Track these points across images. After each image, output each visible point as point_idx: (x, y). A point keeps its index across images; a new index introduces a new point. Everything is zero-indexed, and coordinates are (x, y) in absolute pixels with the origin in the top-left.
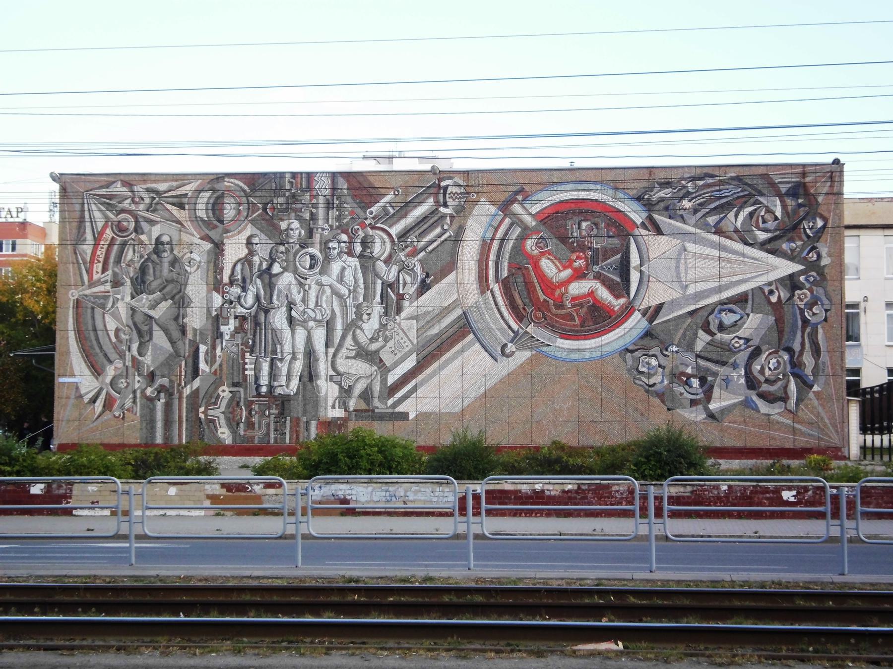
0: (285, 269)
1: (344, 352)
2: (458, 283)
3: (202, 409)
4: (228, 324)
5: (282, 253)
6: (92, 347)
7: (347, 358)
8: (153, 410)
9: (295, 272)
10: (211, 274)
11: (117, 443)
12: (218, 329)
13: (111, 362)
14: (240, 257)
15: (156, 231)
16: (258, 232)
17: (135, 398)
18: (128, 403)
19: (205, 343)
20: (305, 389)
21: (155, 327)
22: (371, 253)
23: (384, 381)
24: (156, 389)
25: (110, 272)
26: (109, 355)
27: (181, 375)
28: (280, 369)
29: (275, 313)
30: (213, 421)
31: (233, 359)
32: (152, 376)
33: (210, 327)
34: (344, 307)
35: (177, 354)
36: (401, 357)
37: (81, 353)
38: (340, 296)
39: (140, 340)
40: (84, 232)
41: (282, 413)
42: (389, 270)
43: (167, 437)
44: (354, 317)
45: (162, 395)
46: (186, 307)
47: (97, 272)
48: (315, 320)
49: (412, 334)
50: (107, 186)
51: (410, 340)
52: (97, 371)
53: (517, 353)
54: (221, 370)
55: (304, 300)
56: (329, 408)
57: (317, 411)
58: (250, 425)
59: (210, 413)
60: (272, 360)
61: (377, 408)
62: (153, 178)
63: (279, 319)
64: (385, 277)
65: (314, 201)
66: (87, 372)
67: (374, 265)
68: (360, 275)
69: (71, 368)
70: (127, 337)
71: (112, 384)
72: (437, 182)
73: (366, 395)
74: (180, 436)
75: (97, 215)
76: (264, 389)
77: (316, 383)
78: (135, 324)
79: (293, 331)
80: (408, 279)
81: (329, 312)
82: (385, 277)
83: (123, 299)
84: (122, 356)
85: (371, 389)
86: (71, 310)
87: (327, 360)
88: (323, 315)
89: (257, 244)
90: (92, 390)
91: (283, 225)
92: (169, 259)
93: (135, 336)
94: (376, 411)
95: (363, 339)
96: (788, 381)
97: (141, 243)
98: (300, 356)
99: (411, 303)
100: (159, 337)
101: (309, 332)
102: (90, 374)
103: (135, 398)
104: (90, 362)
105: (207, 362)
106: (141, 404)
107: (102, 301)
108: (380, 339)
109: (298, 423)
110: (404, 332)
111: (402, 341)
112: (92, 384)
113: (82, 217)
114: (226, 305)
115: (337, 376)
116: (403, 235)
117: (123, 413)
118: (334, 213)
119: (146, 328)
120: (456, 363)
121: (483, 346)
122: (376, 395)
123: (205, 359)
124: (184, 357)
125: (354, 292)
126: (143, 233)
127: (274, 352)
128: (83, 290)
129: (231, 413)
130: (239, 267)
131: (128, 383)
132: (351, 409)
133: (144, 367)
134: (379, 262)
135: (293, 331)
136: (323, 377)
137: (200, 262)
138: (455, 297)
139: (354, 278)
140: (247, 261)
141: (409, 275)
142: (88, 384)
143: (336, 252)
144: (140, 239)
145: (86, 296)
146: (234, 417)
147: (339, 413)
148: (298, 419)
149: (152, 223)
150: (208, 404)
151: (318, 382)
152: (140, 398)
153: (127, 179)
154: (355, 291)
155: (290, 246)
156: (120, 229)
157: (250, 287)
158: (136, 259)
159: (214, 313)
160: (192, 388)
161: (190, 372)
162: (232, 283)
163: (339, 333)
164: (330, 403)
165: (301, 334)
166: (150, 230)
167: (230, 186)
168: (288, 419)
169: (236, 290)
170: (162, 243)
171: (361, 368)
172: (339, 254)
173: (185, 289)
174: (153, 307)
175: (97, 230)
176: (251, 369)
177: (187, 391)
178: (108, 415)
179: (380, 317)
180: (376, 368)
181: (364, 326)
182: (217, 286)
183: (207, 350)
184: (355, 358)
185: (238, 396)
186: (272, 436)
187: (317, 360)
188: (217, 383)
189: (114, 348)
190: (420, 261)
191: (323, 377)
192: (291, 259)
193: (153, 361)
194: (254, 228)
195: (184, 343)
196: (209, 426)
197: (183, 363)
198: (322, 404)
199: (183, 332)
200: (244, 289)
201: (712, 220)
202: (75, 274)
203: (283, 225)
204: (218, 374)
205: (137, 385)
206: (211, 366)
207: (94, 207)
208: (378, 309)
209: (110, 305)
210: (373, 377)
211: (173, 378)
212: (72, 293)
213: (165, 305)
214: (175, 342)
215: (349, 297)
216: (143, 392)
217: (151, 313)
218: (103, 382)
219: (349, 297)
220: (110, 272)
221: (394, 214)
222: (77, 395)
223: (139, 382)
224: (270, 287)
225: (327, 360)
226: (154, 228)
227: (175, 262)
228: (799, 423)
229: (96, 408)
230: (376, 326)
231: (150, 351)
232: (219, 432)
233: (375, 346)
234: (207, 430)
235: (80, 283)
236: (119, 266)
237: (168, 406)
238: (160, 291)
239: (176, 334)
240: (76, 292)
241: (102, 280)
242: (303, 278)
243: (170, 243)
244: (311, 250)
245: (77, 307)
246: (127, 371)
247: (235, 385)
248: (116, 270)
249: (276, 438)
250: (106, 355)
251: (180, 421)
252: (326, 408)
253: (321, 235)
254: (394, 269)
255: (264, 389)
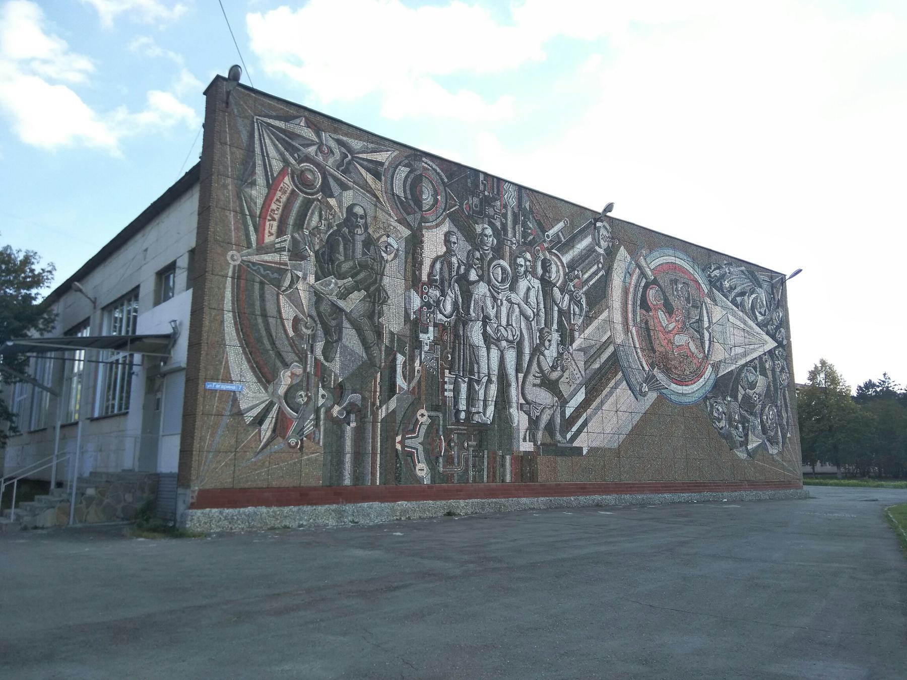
0: (481, 278)
1: (530, 378)
2: (609, 321)
3: (399, 438)
4: (427, 332)
5: (477, 259)
6: (259, 340)
7: (534, 385)
8: (341, 437)
9: (489, 283)
10: (409, 268)
11: (291, 485)
12: (418, 337)
13: (286, 365)
14: (439, 254)
15: (348, 197)
16: (455, 230)
17: (317, 419)
18: (309, 427)
19: (404, 354)
20: (500, 417)
21: (346, 324)
22: (550, 277)
23: (563, 413)
24: (344, 408)
25: (288, 237)
26: (284, 354)
27: (375, 392)
28: (477, 393)
29: (472, 327)
30: (411, 455)
31: (433, 375)
32: (339, 392)
33: (408, 333)
34: (530, 328)
35: (371, 363)
36: (575, 389)
37: (242, 346)
38: (527, 318)
39: (326, 339)
40: (253, 173)
41: (480, 447)
42: (563, 298)
43: (357, 477)
44: (538, 342)
45: (353, 417)
46: (382, 304)
47: (272, 234)
48: (507, 341)
49: (581, 364)
50: (287, 119)
51: (580, 372)
52: (266, 377)
53: (650, 394)
54: (419, 388)
55: (498, 316)
56: (521, 440)
57: (511, 444)
58: (449, 460)
59: (408, 443)
60: (470, 380)
61: (559, 442)
62: (344, 127)
63: (476, 335)
64: (560, 305)
65: (503, 211)
66: (250, 376)
67: (552, 290)
68: (541, 298)
69: (227, 368)
70: (309, 332)
71: (289, 396)
72: (593, 222)
73: (550, 427)
74: (373, 474)
75: (272, 152)
76: (463, 415)
77: (509, 412)
78: (319, 314)
79: (488, 349)
80: (577, 310)
81: (518, 333)
82: (560, 305)
83: (305, 278)
84: (303, 360)
85: (554, 421)
86: (229, 279)
87: (518, 386)
88: (514, 336)
89: (455, 243)
90: (257, 405)
91: (479, 228)
92: (363, 238)
93: (320, 333)
94: (559, 445)
95: (546, 368)
96: (778, 428)
97: (330, 208)
98: (494, 379)
99: (580, 335)
100: (350, 338)
101: (502, 352)
102: (255, 379)
103: (317, 419)
104: (256, 363)
105: (405, 378)
106: (325, 430)
107: (276, 275)
108: (559, 369)
109: (495, 458)
110: (575, 363)
111: (575, 373)
112: (258, 395)
113: (250, 150)
114: (425, 309)
115: (527, 406)
116: (572, 266)
117: (302, 440)
118: (519, 229)
119: (333, 323)
120: (612, 400)
121: (628, 385)
122: (558, 427)
123: (403, 372)
124: (380, 368)
125: (537, 315)
126: (332, 196)
127: (472, 372)
128: (249, 254)
129: (430, 444)
130: (438, 266)
131: (309, 398)
132: (539, 443)
133: (330, 376)
134: (555, 288)
135: (488, 349)
136: (515, 405)
137: (398, 250)
138: (609, 334)
139: (537, 300)
140: (445, 259)
141: (578, 307)
142: (251, 394)
143: (523, 269)
144: (328, 202)
145: (254, 264)
146: (433, 449)
147: (526, 447)
148: (495, 453)
149: (344, 187)
150: (406, 432)
151: (511, 410)
152: (325, 419)
153: (312, 117)
154: (538, 314)
155: (485, 253)
156: (301, 181)
157: (449, 292)
158: (323, 228)
159: (413, 317)
160: (387, 409)
161: (385, 387)
162: (431, 282)
163: (527, 358)
164: (522, 436)
165: (494, 353)
166: (341, 194)
167: (429, 169)
168: (486, 452)
169: (435, 293)
170: (356, 215)
171: (543, 397)
172: (526, 272)
173: (381, 279)
174: (343, 296)
175: (272, 175)
176: (450, 390)
177: (382, 413)
178: (279, 444)
179: (558, 345)
180: (557, 399)
181: (546, 352)
182: (414, 282)
183: (405, 362)
184: (540, 386)
185: (437, 422)
186: (471, 473)
187: (510, 385)
188: (414, 407)
189: (292, 346)
190: (586, 293)
191: (515, 405)
192: (486, 268)
193: (342, 368)
194: (452, 225)
195: (380, 350)
196: (406, 460)
197: (379, 374)
198: (515, 435)
199: (379, 334)
200: (443, 294)
201: (739, 299)
202: (237, 229)
203: (479, 228)
204: (416, 393)
205: (321, 402)
206: (409, 383)
207: (268, 141)
208: (556, 337)
209: (287, 283)
210: (555, 408)
211: (367, 394)
212: (232, 256)
213: (356, 297)
214: (371, 347)
215: (533, 320)
216: (329, 410)
217: (341, 303)
218: (274, 393)
219: (533, 320)
220: (288, 237)
221: (564, 244)
222: (235, 410)
223: (323, 396)
224: (467, 295)
225: (518, 386)
226: (345, 194)
227: (369, 242)
228: (785, 461)
229: (263, 433)
230: (555, 355)
231: (338, 355)
232: (417, 468)
233: (555, 375)
234: (403, 466)
235: (245, 244)
236: (300, 232)
237: (359, 433)
238: (352, 278)
239: (370, 335)
240: (238, 255)
241: (277, 246)
242: (496, 291)
243: (364, 217)
244: (502, 262)
245: (239, 278)
246: (308, 381)
247: (436, 408)
248: (296, 235)
249: (474, 477)
250: (279, 354)
251: (374, 454)
252: (519, 441)
253: (511, 248)
254: (567, 297)
255: (463, 415)
